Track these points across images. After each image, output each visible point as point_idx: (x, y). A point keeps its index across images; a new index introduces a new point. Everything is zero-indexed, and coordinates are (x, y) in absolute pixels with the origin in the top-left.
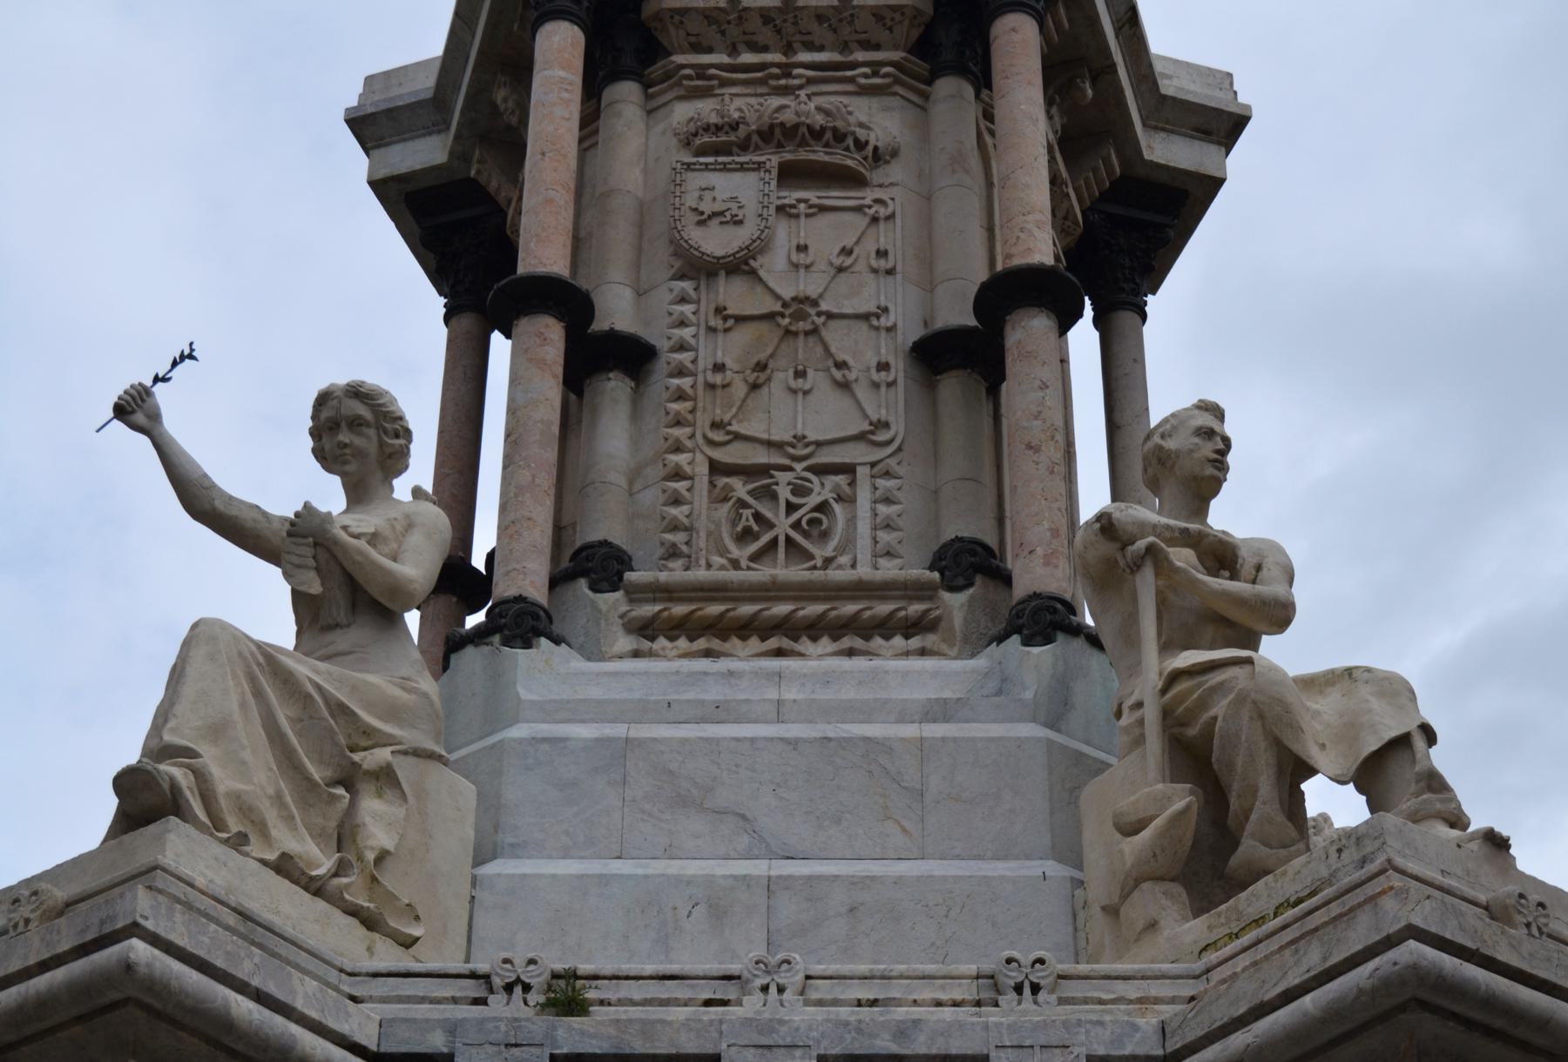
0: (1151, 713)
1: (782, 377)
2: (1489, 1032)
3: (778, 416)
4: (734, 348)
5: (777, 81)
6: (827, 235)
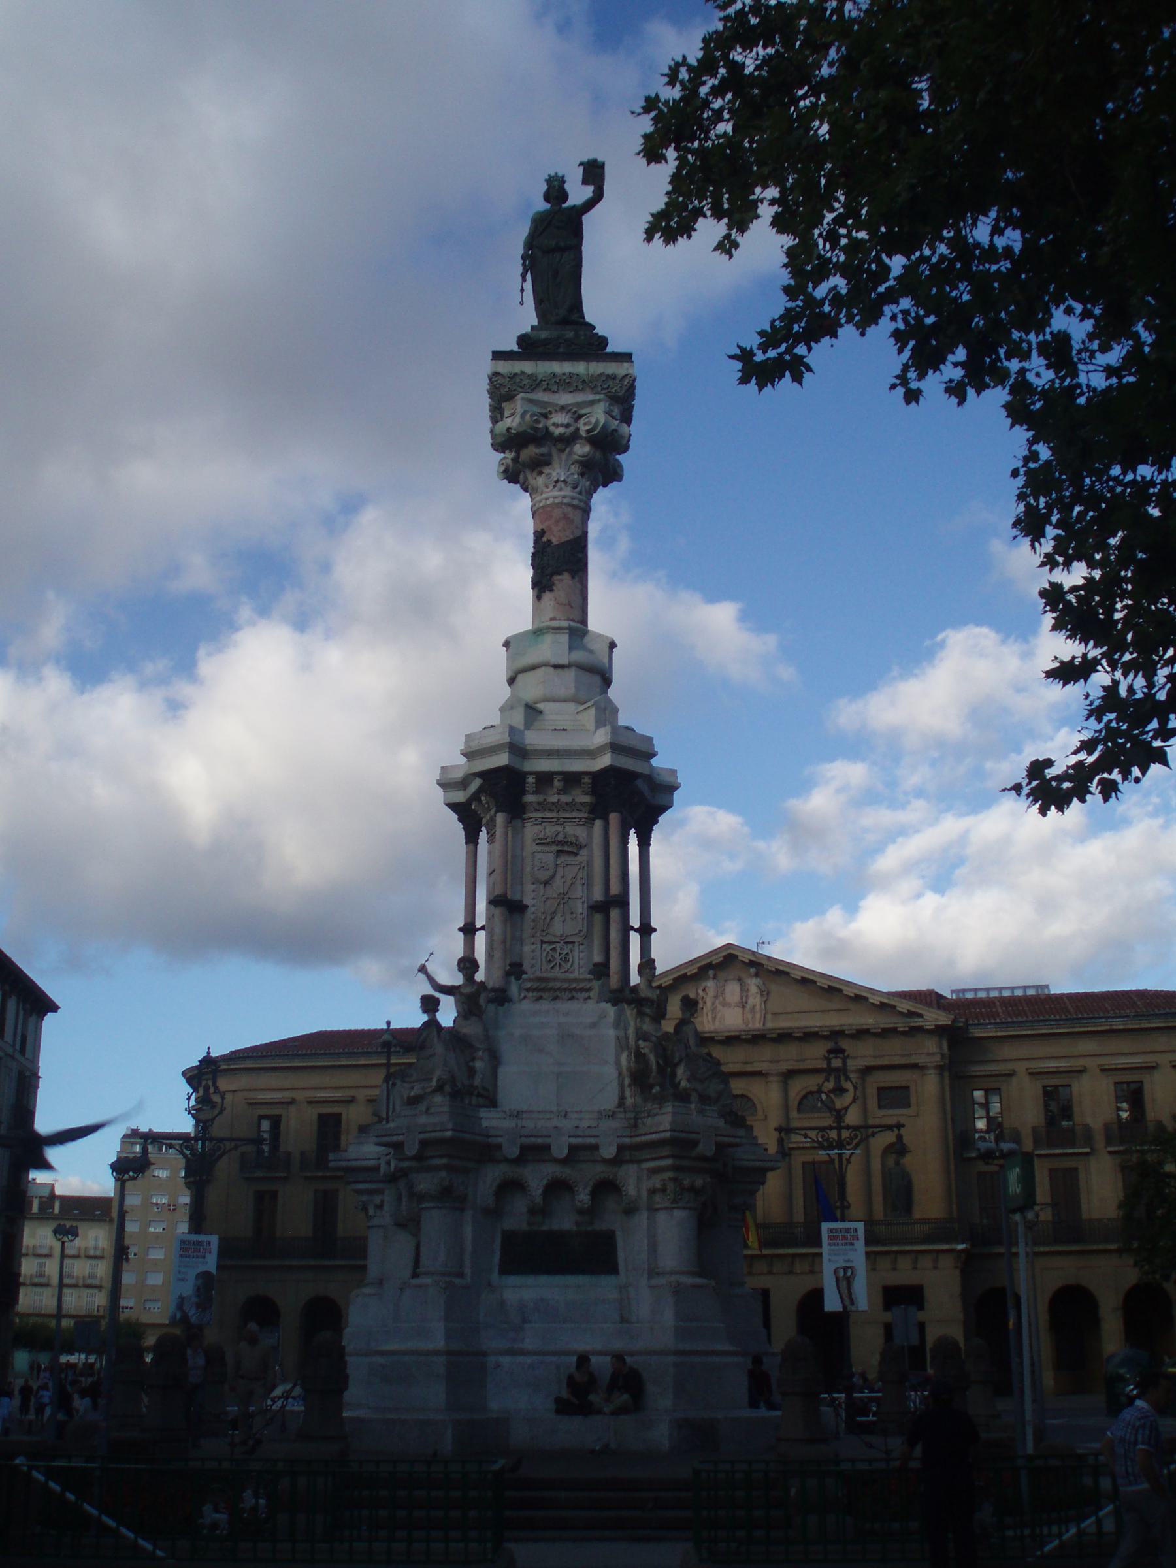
1: (558, 918)
3: (557, 928)
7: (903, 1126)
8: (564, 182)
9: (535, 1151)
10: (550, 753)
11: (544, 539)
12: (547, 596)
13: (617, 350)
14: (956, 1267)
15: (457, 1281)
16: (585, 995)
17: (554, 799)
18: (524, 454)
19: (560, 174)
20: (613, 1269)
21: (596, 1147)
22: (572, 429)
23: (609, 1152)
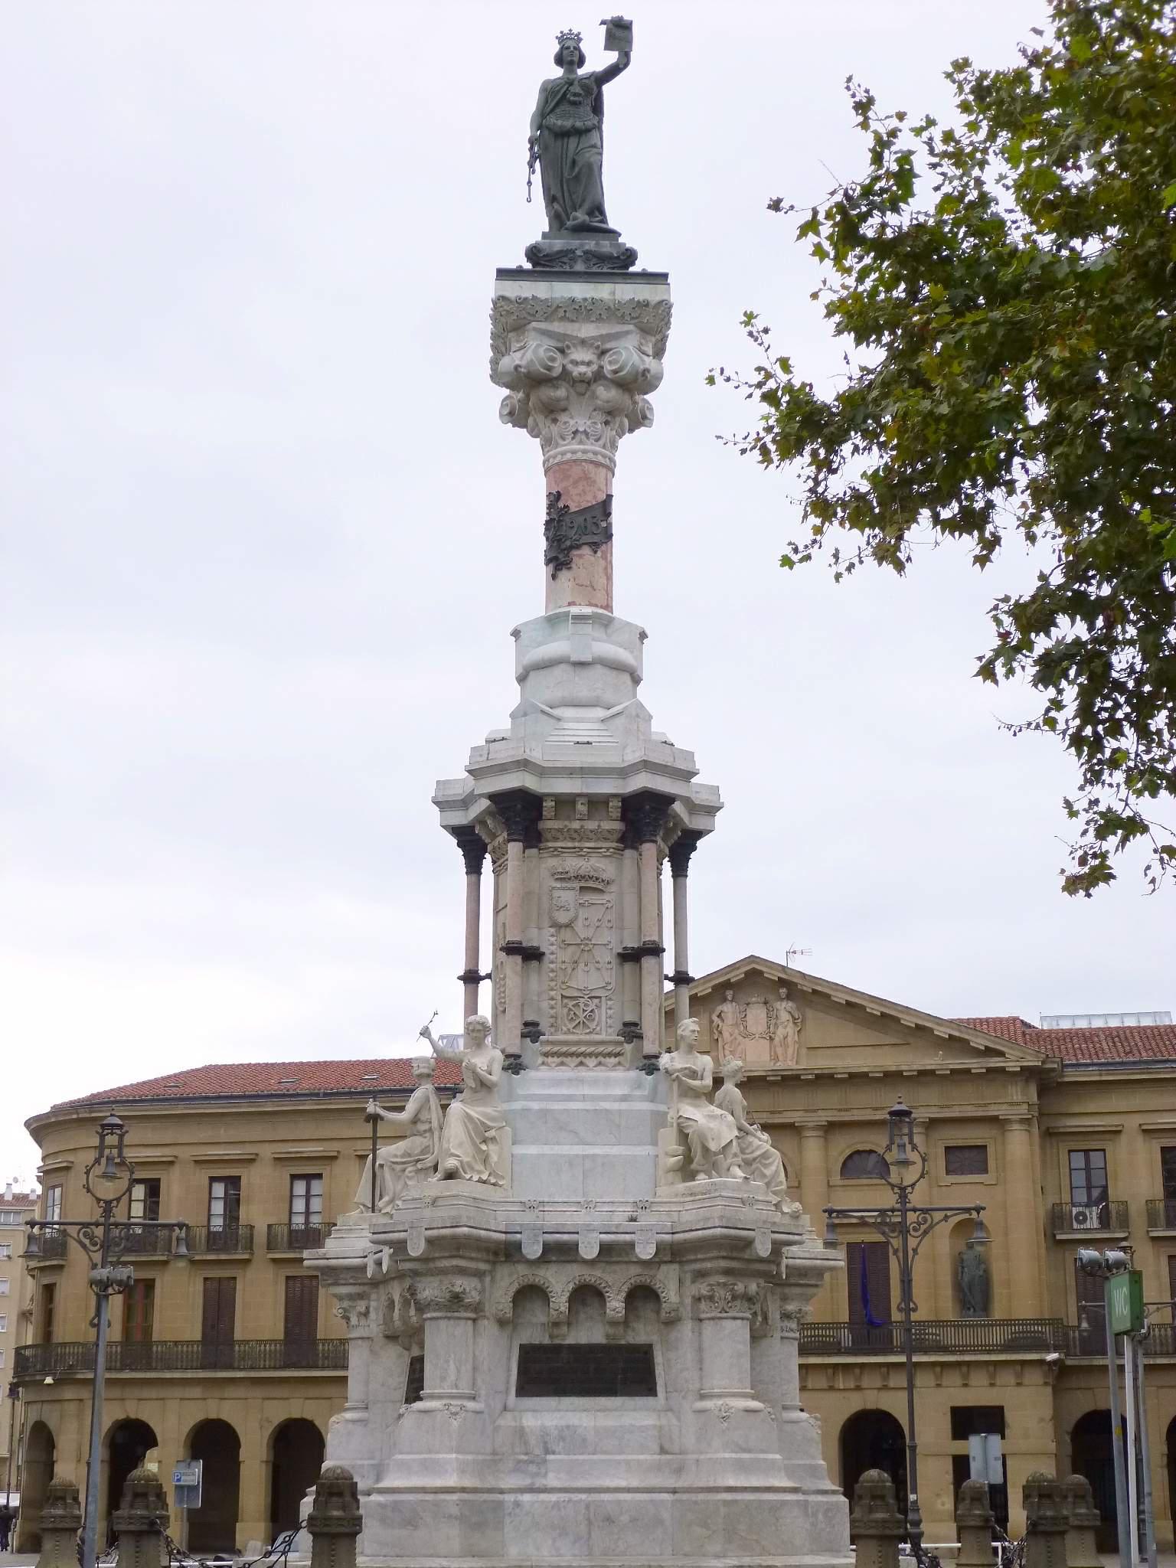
4: (566, 955)
5: (578, 852)
6: (595, 914)
7: (984, 1209)
8: (580, 40)
9: (560, 1252)
10: (571, 772)
11: (561, 505)
12: (564, 575)
13: (650, 270)
14: (1046, 1384)
15: (471, 1405)
16: (613, 1060)
17: (576, 825)
18: (534, 397)
19: (575, 32)
21: (631, 1245)
22: (595, 367)
23: (646, 1252)
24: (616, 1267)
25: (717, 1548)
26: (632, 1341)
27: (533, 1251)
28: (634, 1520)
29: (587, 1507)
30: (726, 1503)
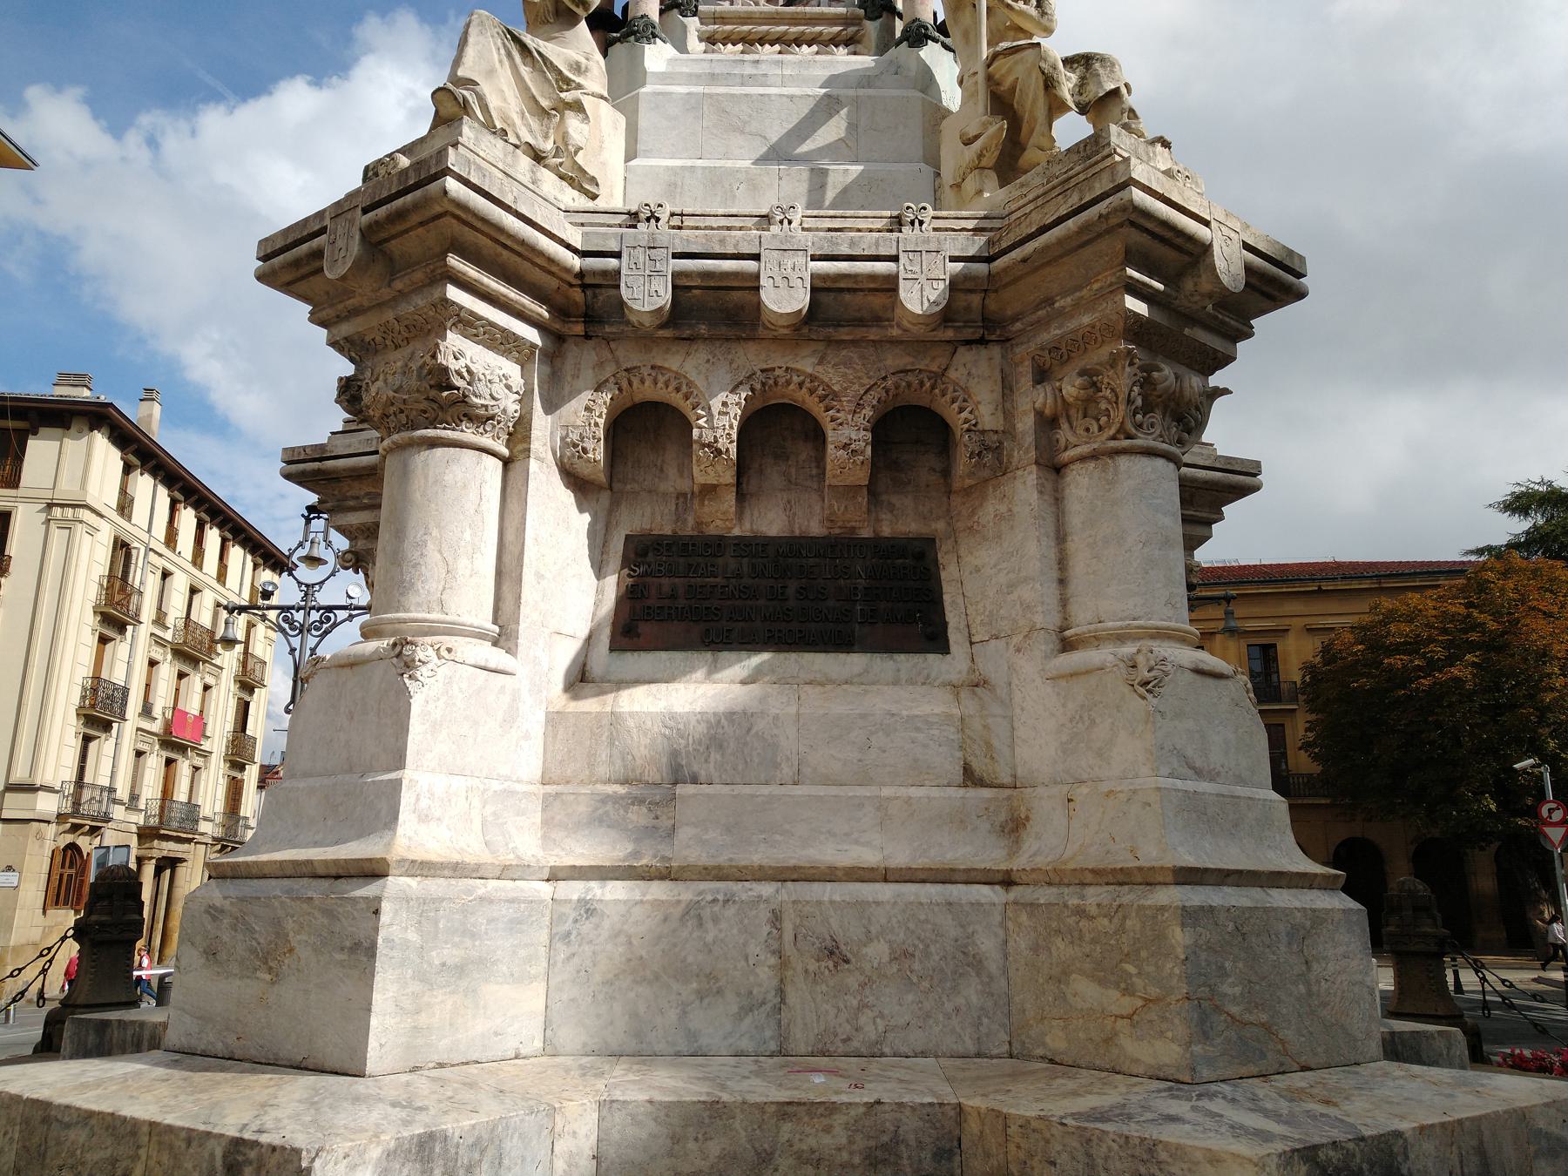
0: (981, 77)
2: (1162, 240)
20: (936, 640)
24: (852, 354)
25: (1167, 1052)
26: (886, 531)
27: (647, 293)
28: (902, 955)
29: (776, 918)
30: (1190, 916)
